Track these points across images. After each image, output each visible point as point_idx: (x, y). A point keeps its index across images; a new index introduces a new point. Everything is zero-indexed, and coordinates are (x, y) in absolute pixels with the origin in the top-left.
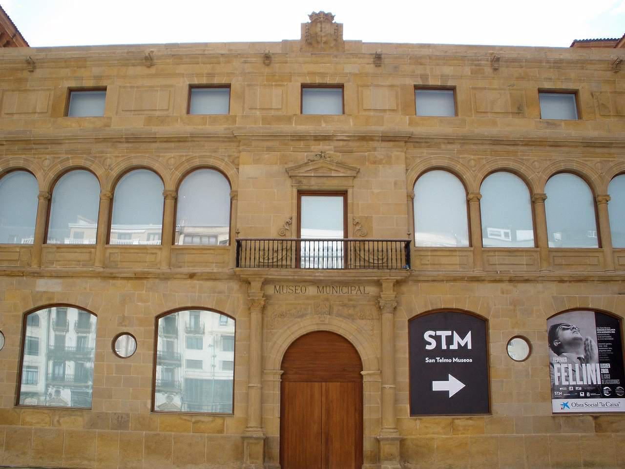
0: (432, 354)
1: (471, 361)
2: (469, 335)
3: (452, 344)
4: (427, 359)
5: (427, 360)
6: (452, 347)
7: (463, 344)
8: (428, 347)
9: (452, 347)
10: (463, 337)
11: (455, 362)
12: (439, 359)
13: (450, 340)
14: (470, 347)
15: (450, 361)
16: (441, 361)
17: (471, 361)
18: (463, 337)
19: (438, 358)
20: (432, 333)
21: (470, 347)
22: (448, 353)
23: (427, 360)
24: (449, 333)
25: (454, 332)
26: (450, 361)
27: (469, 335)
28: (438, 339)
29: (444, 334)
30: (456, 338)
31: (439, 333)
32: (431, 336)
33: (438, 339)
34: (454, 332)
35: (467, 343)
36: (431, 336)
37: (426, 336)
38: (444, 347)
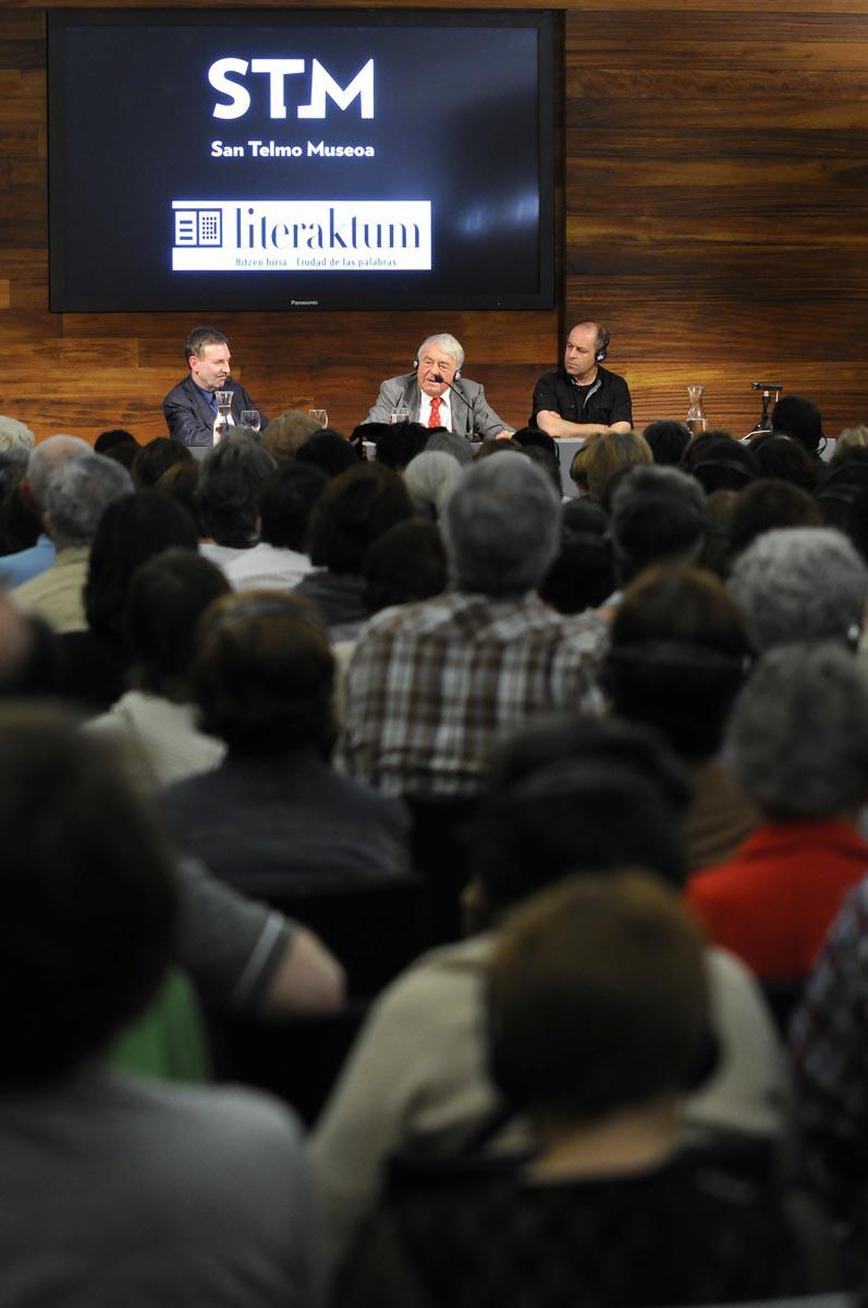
0: (235, 132)
1: (370, 152)
2: (368, 69)
3: (307, 101)
4: (216, 145)
5: (218, 149)
6: (304, 112)
7: (344, 100)
8: (221, 112)
9: (304, 112)
10: (344, 77)
11: (316, 156)
12: (259, 147)
13: (298, 89)
14: (368, 111)
15: (296, 152)
16: (264, 152)
17: (370, 152)
18: (344, 77)
19: (254, 144)
20: (239, 66)
21: (368, 111)
22: (294, 130)
23: (218, 149)
24: (296, 66)
25: (315, 62)
26: (296, 152)
27: (368, 69)
28: (257, 85)
29: (278, 69)
30: (322, 81)
31: (260, 65)
32: (232, 76)
33: (257, 85)
34: (315, 62)
35: (356, 103)
36: (231, 76)
37: (218, 74)
38: (278, 110)
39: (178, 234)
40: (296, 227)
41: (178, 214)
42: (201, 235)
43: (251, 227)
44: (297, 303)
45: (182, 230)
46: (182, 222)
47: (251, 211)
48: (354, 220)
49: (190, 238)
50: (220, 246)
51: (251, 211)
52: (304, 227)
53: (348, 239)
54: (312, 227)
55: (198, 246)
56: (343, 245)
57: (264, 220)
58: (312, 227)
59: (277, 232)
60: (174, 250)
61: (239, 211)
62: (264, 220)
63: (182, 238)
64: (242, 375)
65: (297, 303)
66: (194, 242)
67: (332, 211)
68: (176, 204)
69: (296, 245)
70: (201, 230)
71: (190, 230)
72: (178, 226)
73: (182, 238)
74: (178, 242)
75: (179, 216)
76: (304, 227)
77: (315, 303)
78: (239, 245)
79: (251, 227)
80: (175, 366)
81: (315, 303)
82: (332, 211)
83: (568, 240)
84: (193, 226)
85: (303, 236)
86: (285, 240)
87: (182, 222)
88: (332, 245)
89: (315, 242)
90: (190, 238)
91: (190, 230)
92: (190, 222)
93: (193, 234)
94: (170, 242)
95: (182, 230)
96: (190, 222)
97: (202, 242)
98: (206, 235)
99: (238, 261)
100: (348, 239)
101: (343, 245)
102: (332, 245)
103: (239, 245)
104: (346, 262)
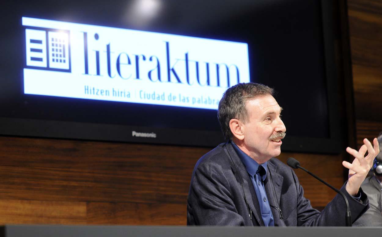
39: (29, 54)
40: (137, 58)
41: (28, 31)
42: (51, 58)
43: (98, 53)
44: (138, 135)
45: (33, 50)
46: (32, 41)
47: (97, 37)
48: (187, 55)
49: (40, 60)
50: (69, 71)
51: (97, 37)
52: (144, 58)
53: (182, 76)
54: (151, 59)
55: (48, 69)
56: (179, 81)
57: (108, 47)
58: (151, 59)
59: (121, 61)
60: (26, 71)
61: (85, 34)
62: (108, 47)
63: (33, 59)
64: (88, 211)
65: (138, 135)
66: (44, 64)
67: (167, 44)
68: (26, 21)
69: (138, 77)
70: (51, 53)
71: (40, 51)
72: (29, 46)
73: (33, 59)
74: (29, 62)
75: (30, 35)
76: (144, 58)
77: (153, 135)
78: (87, 72)
79: (98, 53)
80: (22, 199)
81: (153, 135)
82: (167, 44)
83: (355, 87)
84: (43, 47)
85: (145, 67)
86: (128, 70)
87: (32, 41)
88: (169, 80)
89: (154, 75)
90: (40, 60)
91: (40, 51)
92: (39, 42)
93: (43, 55)
94: (19, 64)
95: (33, 50)
96: (39, 42)
97: (52, 65)
98: (55, 58)
99: (87, 89)
100: (182, 76)
101: (179, 81)
102: (169, 80)
103: (87, 72)
104: (182, 98)
